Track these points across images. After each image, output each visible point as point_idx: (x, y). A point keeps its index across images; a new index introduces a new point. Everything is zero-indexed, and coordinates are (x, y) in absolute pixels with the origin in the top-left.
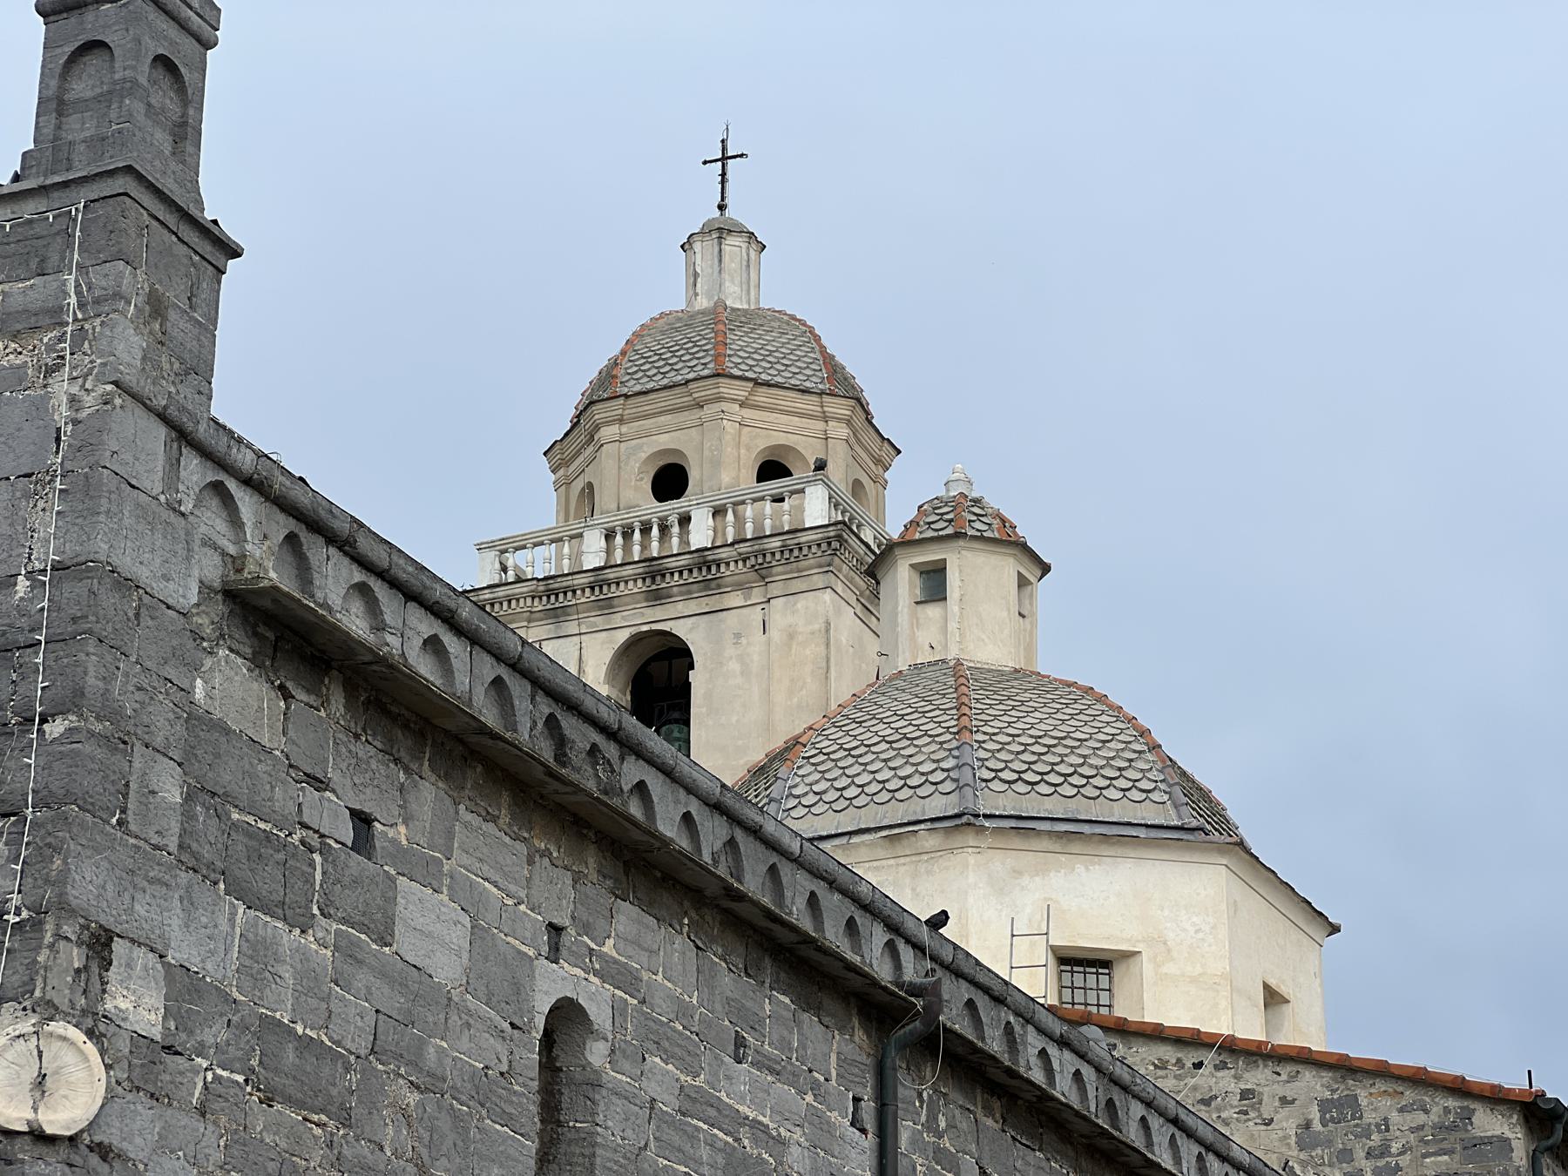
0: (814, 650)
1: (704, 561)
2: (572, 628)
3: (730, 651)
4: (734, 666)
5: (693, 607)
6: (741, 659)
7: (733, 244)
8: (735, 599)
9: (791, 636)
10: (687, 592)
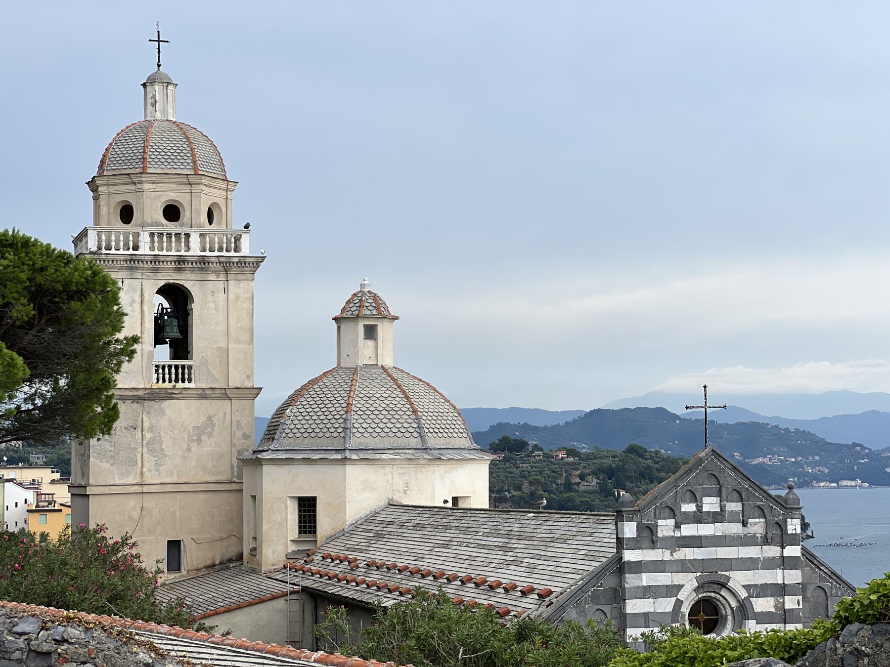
0: (246, 305)
1: (203, 260)
2: (139, 275)
3: (210, 298)
4: (212, 305)
5: (193, 277)
6: (214, 302)
7: (170, 87)
8: (212, 277)
9: (238, 298)
10: (192, 271)
